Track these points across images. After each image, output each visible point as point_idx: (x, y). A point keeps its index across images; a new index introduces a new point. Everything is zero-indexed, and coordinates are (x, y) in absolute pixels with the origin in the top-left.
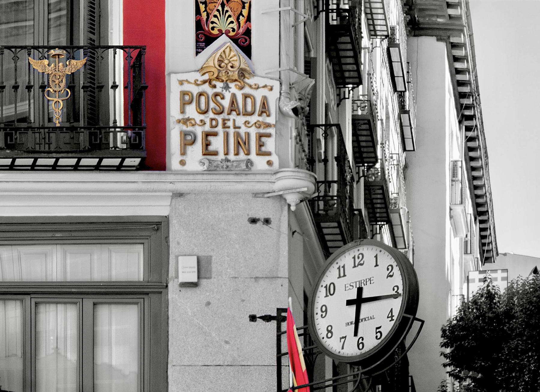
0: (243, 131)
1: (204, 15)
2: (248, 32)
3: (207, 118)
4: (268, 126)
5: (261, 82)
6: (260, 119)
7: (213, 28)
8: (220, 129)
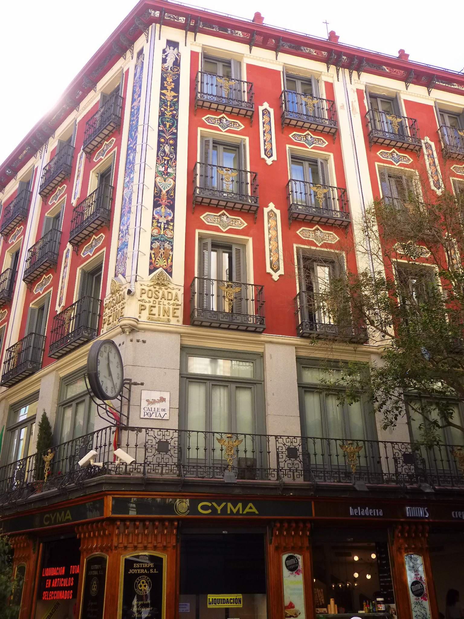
0: (167, 307)
1: (154, 259)
2: (171, 266)
3: (152, 300)
4: (178, 305)
5: (175, 287)
6: (175, 302)
8: (157, 305)
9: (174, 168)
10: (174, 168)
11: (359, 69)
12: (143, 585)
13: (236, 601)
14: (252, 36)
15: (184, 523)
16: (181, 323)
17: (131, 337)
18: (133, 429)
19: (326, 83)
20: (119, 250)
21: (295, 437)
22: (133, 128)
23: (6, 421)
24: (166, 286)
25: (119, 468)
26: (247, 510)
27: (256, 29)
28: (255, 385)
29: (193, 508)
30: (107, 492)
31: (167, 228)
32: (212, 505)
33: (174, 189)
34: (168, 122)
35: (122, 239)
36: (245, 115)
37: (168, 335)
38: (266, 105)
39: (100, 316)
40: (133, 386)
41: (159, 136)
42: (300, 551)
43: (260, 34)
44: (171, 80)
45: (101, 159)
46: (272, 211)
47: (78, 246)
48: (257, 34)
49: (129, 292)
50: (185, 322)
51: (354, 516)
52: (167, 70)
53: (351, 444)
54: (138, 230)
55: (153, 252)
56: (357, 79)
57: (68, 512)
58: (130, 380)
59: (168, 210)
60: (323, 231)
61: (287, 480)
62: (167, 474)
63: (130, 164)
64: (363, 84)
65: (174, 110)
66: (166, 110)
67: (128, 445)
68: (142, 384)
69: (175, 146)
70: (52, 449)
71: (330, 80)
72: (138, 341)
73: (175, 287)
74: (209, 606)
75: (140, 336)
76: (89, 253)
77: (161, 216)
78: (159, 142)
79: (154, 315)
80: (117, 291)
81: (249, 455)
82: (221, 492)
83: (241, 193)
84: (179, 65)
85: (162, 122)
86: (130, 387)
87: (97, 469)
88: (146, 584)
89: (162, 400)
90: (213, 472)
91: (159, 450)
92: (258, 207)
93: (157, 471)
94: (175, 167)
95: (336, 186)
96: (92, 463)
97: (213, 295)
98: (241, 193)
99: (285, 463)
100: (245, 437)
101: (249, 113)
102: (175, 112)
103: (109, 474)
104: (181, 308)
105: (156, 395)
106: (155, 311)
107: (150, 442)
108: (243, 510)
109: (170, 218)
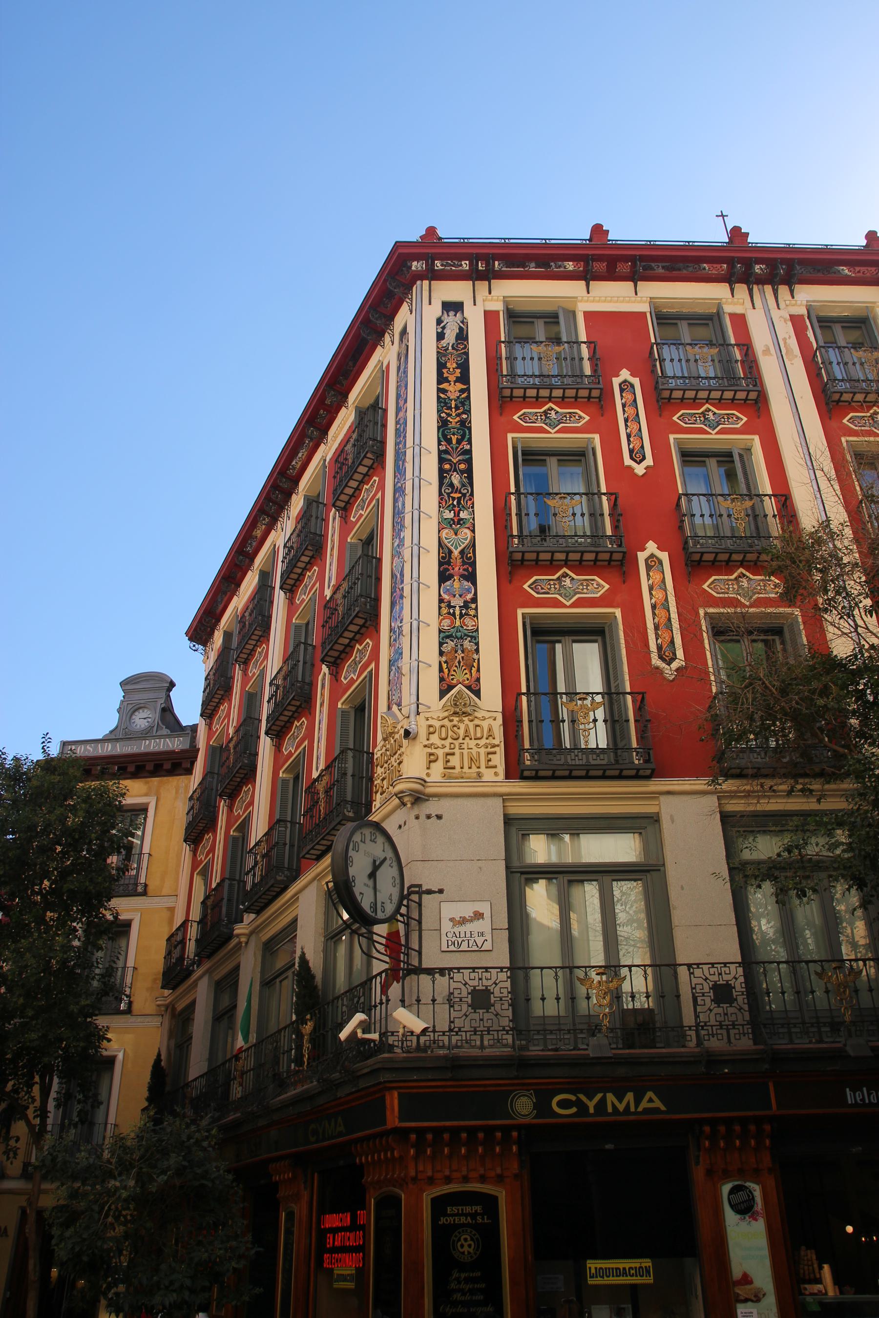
0: (475, 750)
1: (446, 671)
2: (478, 680)
4: (494, 746)
5: (487, 715)
6: (488, 741)
7: (453, 679)
9: (471, 510)
10: (471, 510)
11: (790, 281)
12: (466, 1244)
13: (640, 1272)
14: (586, 265)
15: (529, 1134)
16: (501, 776)
17: (416, 811)
18: (430, 971)
19: (732, 316)
20: (391, 663)
21: (725, 964)
22: (400, 456)
23: (259, 969)
24: (470, 715)
25: (406, 1041)
26: (644, 1104)
27: (590, 252)
28: (648, 872)
29: (542, 1107)
30: (388, 1085)
31: (466, 614)
32: (578, 1099)
33: (474, 546)
34: (454, 434)
35: (394, 645)
36: (589, 397)
37: (481, 801)
38: (625, 374)
39: (371, 780)
40: (424, 896)
41: (441, 461)
42: (756, 1175)
43: (599, 258)
44: (455, 365)
45: (361, 515)
46: (652, 556)
47: (336, 666)
48: (601, 258)
49: (407, 733)
50: (508, 776)
51: (856, 1104)
52: (448, 349)
53: (839, 968)
54: (415, 624)
55: (444, 659)
56: (790, 298)
57: (340, 1120)
58: (420, 886)
59: (466, 583)
60: (751, 576)
61: (714, 1044)
62: (491, 1046)
63: (398, 513)
64: (801, 305)
65: (463, 413)
66: (449, 415)
67: (418, 1001)
68: (441, 891)
69: (469, 473)
70: (311, 1014)
71: (738, 310)
72: (429, 817)
73: (487, 715)
74: (591, 1282)
75: (432, 807)
76: (352, 675)
77: (454, 596)
78: (442, 472)
79: (454, 768)
80: (391, 734)
81: (641, 1003)
82: (585, 1074)
83: (597, 535)
84: (466, 339)
85: (445, 436)
86: (420, 898)
87: (372, 1045)
88: (472, 1243)
89: (478, 916)
90: (576, 1038)
91: (474, 1006)
92: (624, 553)
93: (473, 1043)
94: (473, 507)
95: (770, 492)
96: (360, 1034)
97: (563, 721)
98: (597, 535)
99: (711, 1012)
100: (630, 971)
101: (596, 393)
102: (464, 416)
103: (390, 1052)
104: (500, 751)
105: (467, 910)
106: (455, 761)
107: (456, 992)
108: (636, 1107)
109: (469, 597)
